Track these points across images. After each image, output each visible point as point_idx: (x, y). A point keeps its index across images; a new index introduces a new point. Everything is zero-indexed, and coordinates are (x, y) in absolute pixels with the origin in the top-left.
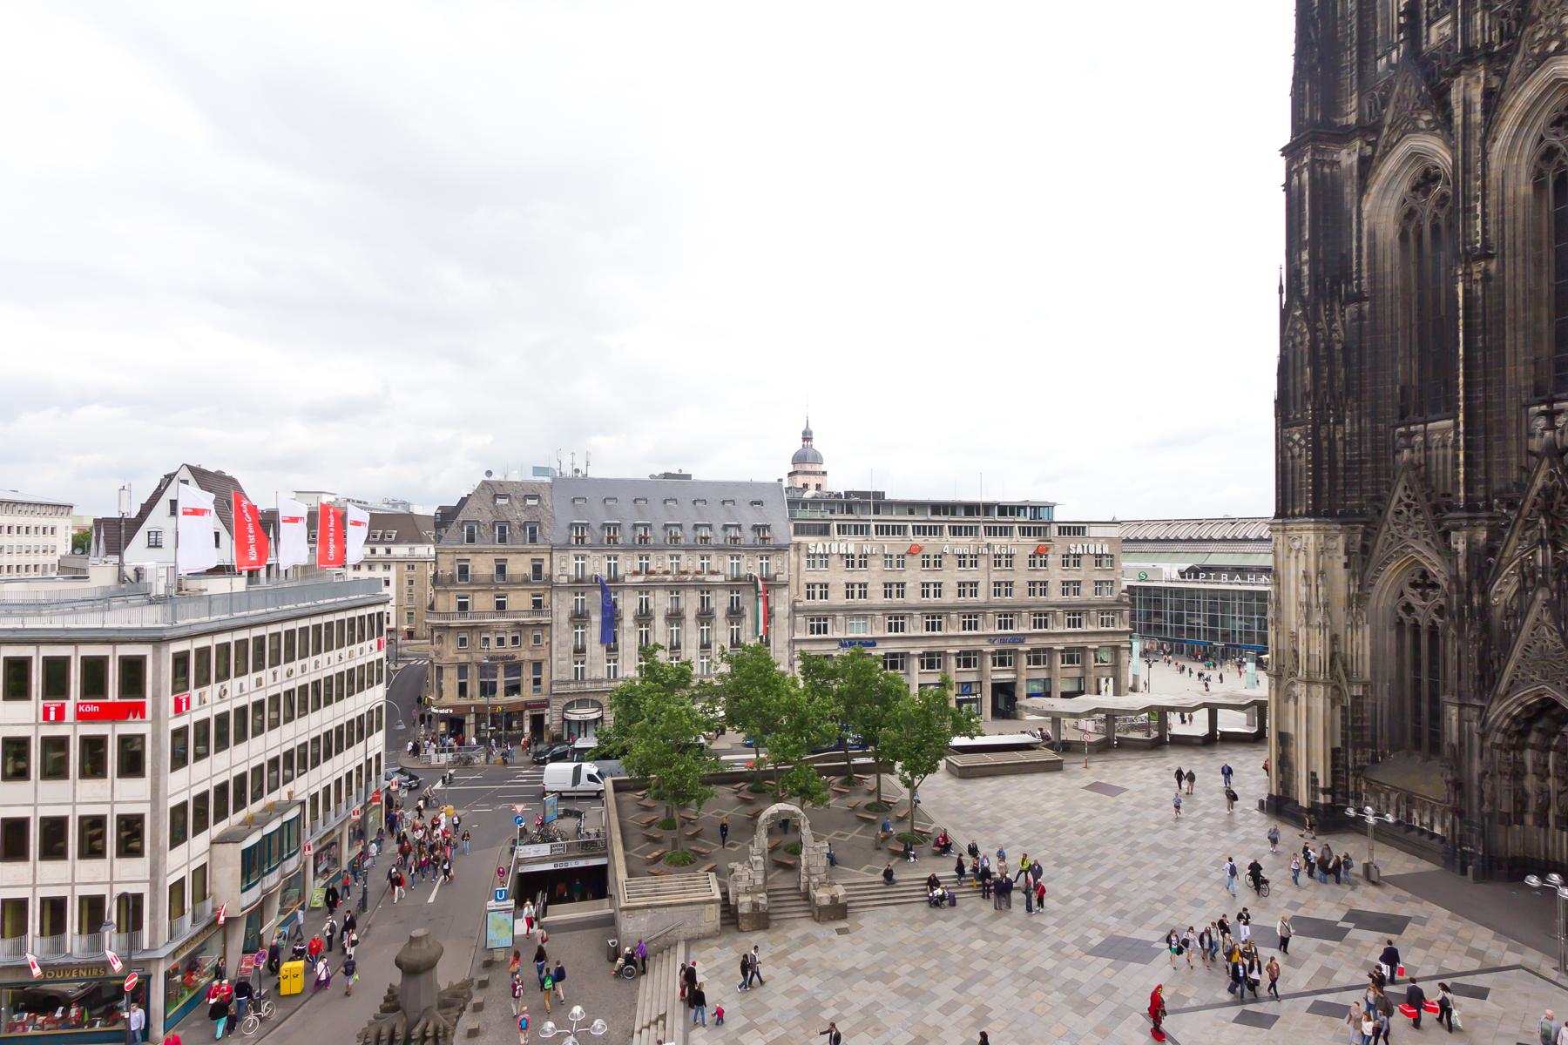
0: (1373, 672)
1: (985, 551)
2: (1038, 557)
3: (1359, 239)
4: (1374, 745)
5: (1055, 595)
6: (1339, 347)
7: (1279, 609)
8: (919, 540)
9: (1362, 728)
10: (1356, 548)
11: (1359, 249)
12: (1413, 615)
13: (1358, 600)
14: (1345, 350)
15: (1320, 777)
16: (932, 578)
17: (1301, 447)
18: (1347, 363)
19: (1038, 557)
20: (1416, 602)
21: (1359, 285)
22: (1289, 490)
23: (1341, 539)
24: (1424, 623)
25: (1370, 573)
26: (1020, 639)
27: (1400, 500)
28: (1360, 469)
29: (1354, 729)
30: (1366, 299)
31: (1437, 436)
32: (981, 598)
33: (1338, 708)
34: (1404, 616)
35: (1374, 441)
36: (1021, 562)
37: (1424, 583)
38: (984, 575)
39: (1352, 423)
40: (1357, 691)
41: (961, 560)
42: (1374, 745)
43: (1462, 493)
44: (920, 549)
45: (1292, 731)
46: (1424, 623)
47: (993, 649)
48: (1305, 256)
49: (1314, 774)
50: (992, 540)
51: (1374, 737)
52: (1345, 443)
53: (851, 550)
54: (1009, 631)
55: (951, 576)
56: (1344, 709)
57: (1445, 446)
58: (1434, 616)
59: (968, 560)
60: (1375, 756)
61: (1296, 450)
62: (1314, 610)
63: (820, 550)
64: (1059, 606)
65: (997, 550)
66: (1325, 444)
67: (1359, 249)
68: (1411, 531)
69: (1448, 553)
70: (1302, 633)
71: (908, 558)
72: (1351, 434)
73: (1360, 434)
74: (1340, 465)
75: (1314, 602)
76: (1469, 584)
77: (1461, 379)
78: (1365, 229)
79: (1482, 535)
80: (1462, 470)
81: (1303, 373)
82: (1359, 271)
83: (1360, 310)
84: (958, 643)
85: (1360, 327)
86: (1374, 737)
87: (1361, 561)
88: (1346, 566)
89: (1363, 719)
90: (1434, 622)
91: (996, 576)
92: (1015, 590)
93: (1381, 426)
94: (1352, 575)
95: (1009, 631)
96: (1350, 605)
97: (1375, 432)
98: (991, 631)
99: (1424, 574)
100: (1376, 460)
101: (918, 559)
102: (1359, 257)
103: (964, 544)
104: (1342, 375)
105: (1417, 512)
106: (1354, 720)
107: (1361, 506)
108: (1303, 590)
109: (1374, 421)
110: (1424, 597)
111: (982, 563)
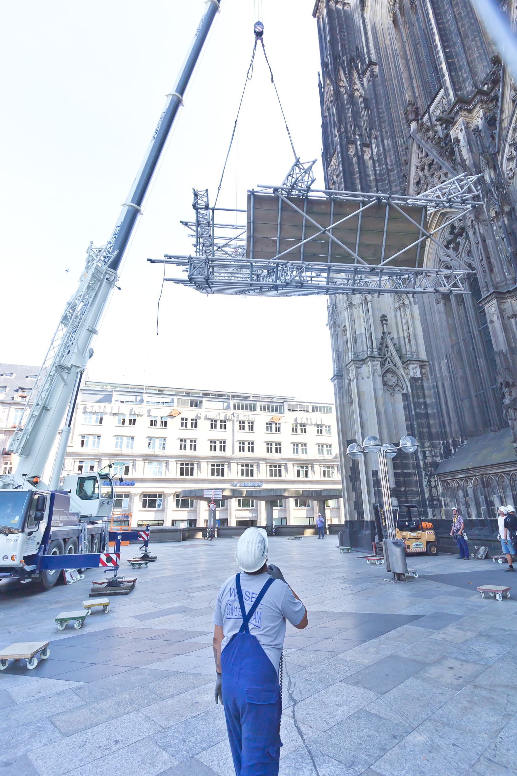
0: (429, 352)
1: (231, 417)
2: (273, 426)
4: (443, 435)
6: (361, 100)
9: (427, 416)
14: (365, 100)
18: (367, 108)
19: (273, 426)
28: (389, 175)
33: (399, 397)
39: (378, 146)
40: (415, 372)
50: (237, 411)
51: (442, 425)
52: (374, 161)
56: (405, 396)
59: (218, 423)
66: (355, 160)
72: (378, 155)
74: (372, 178)
86: (442, 425)
89: (426, 405)
93: (400, 141)
101: (178, 421)
104: (365, 117)
106: (417, 405)
109: (393, 137)
111: (229, 424)
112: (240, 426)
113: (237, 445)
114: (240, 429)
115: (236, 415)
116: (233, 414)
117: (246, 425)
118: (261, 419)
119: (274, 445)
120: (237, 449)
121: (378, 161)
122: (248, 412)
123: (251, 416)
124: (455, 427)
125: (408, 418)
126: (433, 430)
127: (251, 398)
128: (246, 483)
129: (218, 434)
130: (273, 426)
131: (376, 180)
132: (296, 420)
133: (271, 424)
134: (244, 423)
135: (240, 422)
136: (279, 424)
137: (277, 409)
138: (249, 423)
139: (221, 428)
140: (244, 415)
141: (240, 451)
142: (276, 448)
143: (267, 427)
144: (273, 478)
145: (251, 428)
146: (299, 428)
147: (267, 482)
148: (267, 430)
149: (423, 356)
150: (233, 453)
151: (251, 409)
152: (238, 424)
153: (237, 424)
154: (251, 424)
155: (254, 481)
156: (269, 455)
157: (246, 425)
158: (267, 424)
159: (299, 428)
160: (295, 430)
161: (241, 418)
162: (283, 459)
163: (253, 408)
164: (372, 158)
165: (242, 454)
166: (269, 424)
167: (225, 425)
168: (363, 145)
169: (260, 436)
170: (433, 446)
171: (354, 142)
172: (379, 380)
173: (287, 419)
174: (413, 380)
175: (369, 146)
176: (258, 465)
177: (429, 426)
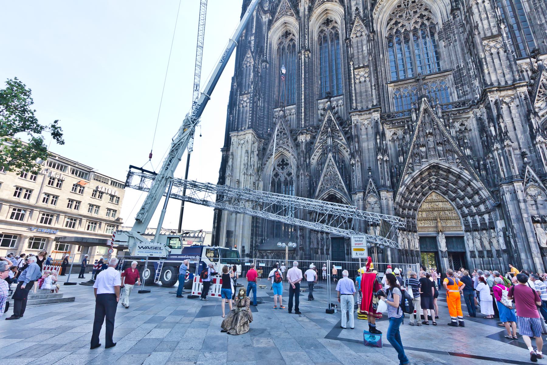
2: (78, 188)
4: (262, 236)
5: (83, 210)
7: (232, 170)
10: (261, 147)
11: (267, 46)
12: (279, 177)
13: (260, 169)
15: (246, 248)
17: (247, 103)
20: (280, 172)
21: (266, 58)
22: (240, 120)
24: (283, 179)
25: (265, 159)
27: (278, 130)
28: (263, 120)
31: (288, 112)
32: (32, 201)
34: (275, 178)
35: (268, 111)
37: (283, 164)
42: (262, 236)
43: (303, 123)
45: (232, 229)
46: (283, 179)
47: (32, 235)
48: (253, 38)
49: (243, 247)
50: (51, 169)
51: (262, 231)
54: (47, 225)
57: (290, 115)
58: (286, 176)
60: (262, 240)
61: (245, 104)
62: (249, 168)
64: (85, 216)
67: (267, 46)
68: (281, 142)
69: (297, 145)
70: (242, 180)
72: (261, 107)
73: (264, 107)
75: (249, 164)
76: (306, 155)
77: (303, 85)
79: (308, 138)
80: (303, 114)
81: (250, 74)
82: (266, 53)
83: (266, 66)
86: (262, 231)
87: (263, 153)
88: (258, 155)
90: (286, 178)
92: (59, 202)
94: (259, 159)
96: (258, 171)
97: (268, 108)
99: (283, 161)
100: (268, 118)
102: (267, 49)
105: (285, 134)
107: (262, 133)
108: (246, 158)
109: (268, 104)
110: (283, 169)
111: (40, 178)
112: (50, 181)
113: (43, 196)
114: (49, 184)
115: (49, 171)
116: (47, 170)
117: (56, 181)
118: (70, 180)
119: (75, 202)
120: (41, 199)
122: (59, 171)
123: (62, 176)
124: (266, 233)
127: (57, 158)
128: (43, 229)
130: (79, 188)
132: (97, 187)
133: (76, 186)
134: (54, 179)
135: (51, 178)
136: (84, 188)
137: (82, 175)
138: (59, 181)
139: (31, 179)
140: (55, 172)
141: (43, 201)
142: (76, 205)
143: (73, 188)
144: (68, 228)
145: (59, 185)
146: (98, 193)
147: (62, 230)
148: (73, 190)
150: (37, 202)
151: (61, 170)
152: (49, 179)
153: (48, 179)
154: (60, 182)
155: (51, 228)
156: (68, 210)
157: (56, 181)
158: (74, 185)
159: (98, 193)
160: (94, 195)
161: (53, 175)
162: (81, 215)
163: (62, 168)
165: (44, 205)
166: (76, 186)
167: (35, 177)
169: (65, 194)
173: (91, 185)
176: (58, 217)
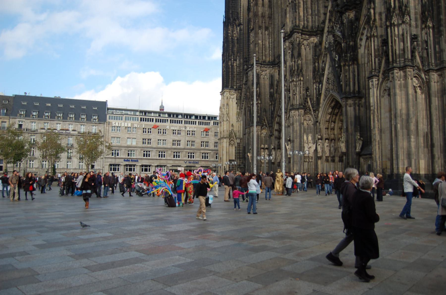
3: (241, 8)
6: (236, 38)
8: (158, 124)
14: (237, 39)
16: (162, 138)
18: (237, 43)
23: (235, 96)
26: (197, 162)
29: (238, 153)
30: (241, 25)
33: (234, 147)
36: (198, 134)
38: (183, 139)
40: (238, 141)
41: (174, 132)
44: (158, 127)
50: (186, 125)
53: (129, 125)
54: (192, 159)
55: (170, 138)
56: (235, 147)
63: (117, 125)
65: (188, 129)
71: (152, 129)
78: (242, 5)
84: (171, 162)
85: (240, 33)
88: (237, 103)
89: (240, 150)
91: (188, 139)
95: (192, 159)
98: (185, 159)
101: (156, 130)
103: (176, 126)
106: (238, 150)
111: (183, 133)
121: (238, 67)
125: (235, 153)
126: (241, 157)
129: (177, 137)
131: (237, 75)
149: (241, 137)
164: (236, 65)
168: (234, 60)
170: (240, 161)
171: (231, 60)
172: (228, 144)
174: (238, 143)
175: (236, 60)
177: (240, 155)
